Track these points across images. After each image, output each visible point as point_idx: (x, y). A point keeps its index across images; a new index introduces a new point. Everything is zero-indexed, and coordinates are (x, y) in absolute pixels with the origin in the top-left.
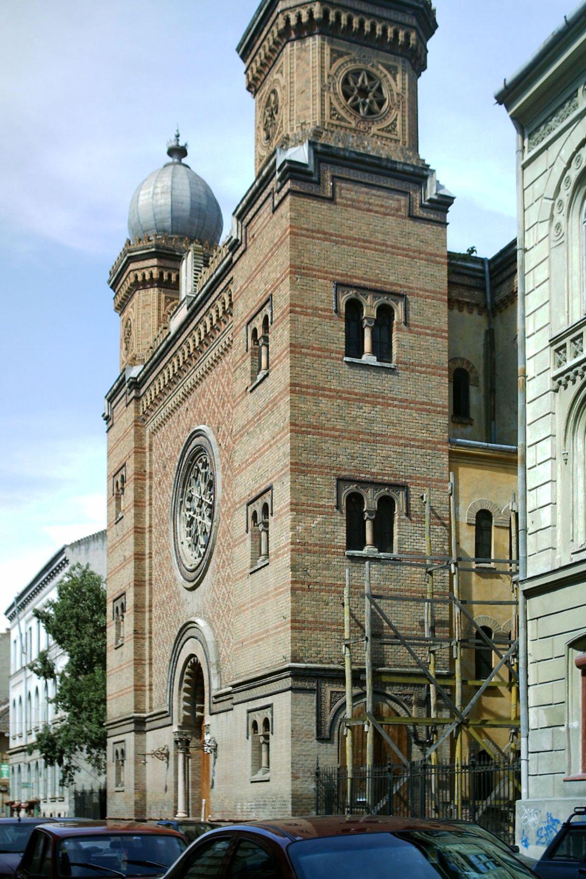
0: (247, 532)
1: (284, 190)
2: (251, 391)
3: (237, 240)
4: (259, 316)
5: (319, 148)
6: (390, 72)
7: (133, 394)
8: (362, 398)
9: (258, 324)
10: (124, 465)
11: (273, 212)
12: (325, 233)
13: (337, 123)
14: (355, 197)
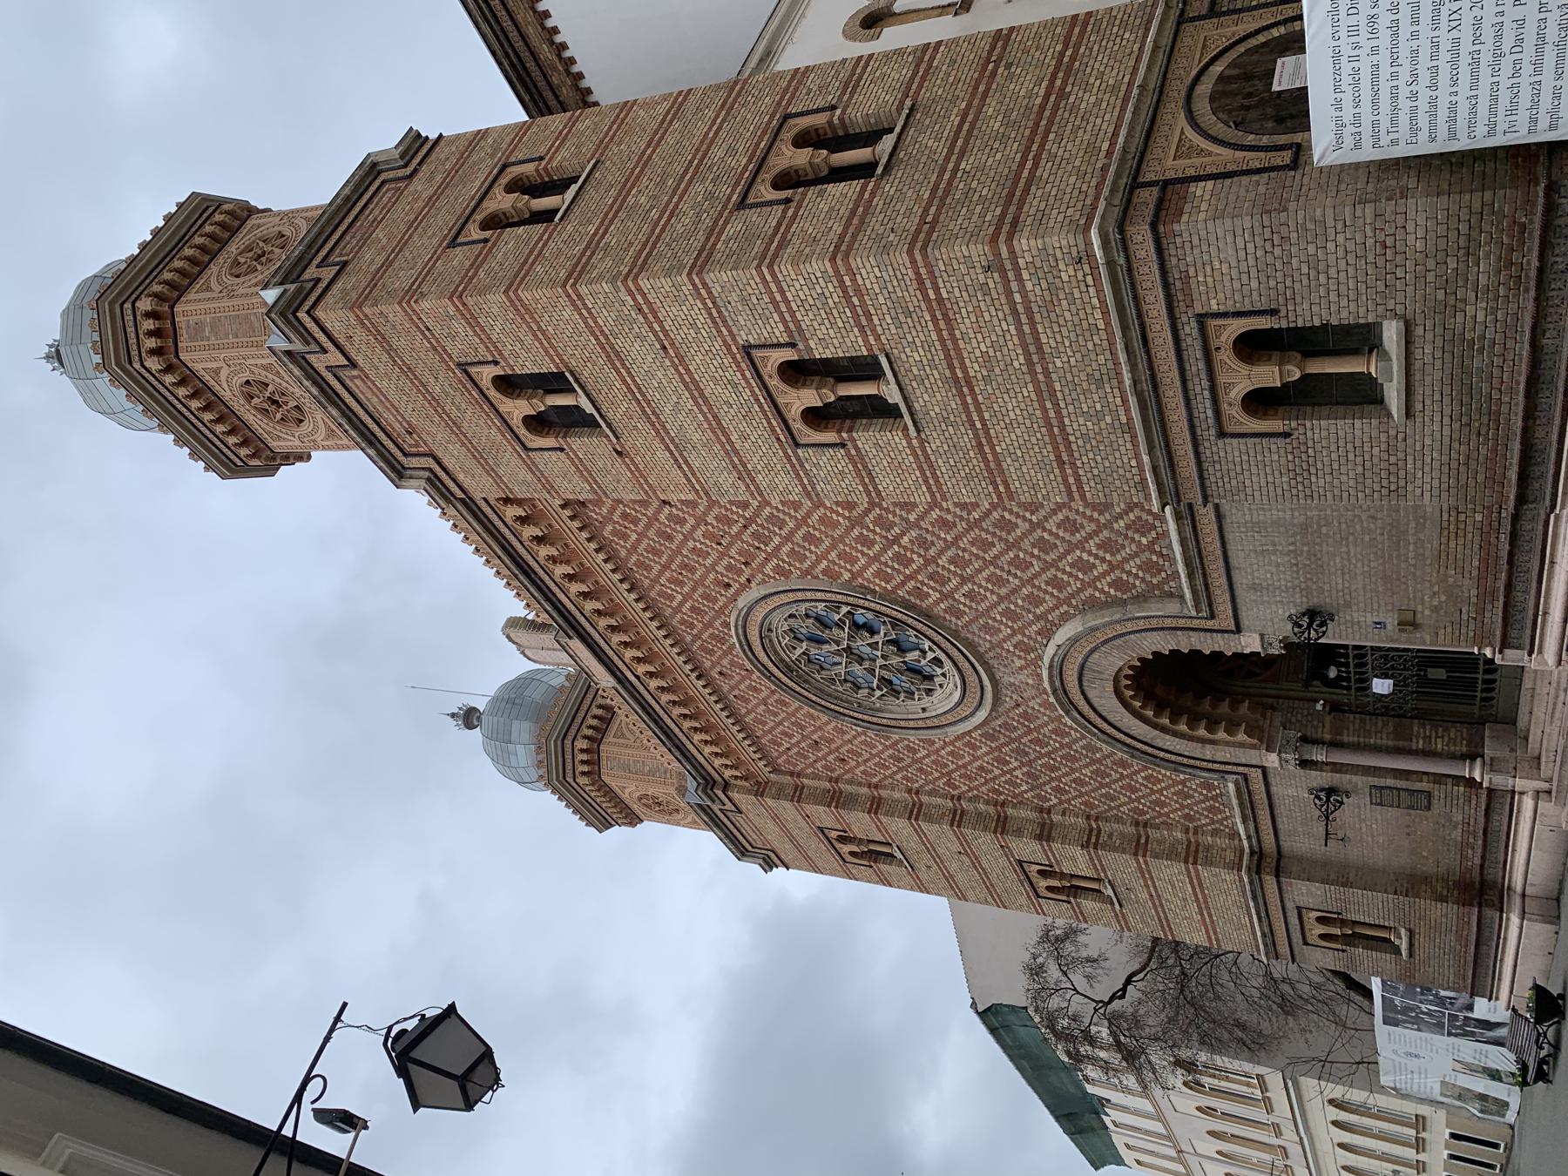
3: (429, 480)
7: (720, 793)
10: (821, 829)
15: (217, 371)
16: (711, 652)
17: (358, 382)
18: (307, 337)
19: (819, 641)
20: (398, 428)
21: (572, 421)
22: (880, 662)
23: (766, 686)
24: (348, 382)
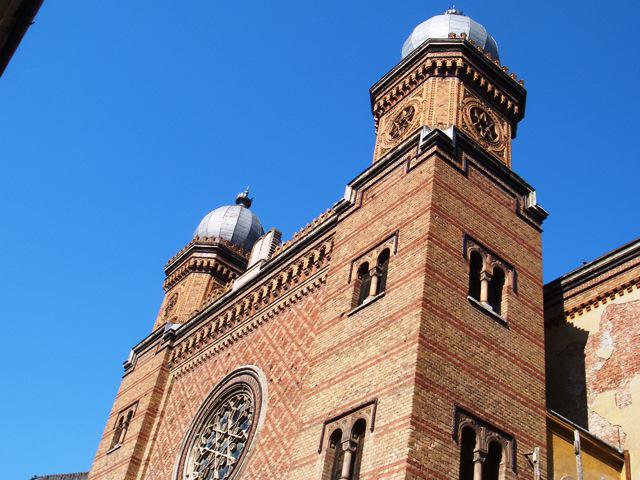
2: (349, 316)
3: (349, 203)
4: (375, 252)
7: (168, 343)
10: (137, 402)
15: (421, 95)
16: (241, 351)
17: (400, 173)
18: (424, 149)
19: (234, 419)
20: (376, 190)
21: (362, 291)
22: (217, 453)
23: (217, 380)
24: (401, 166)
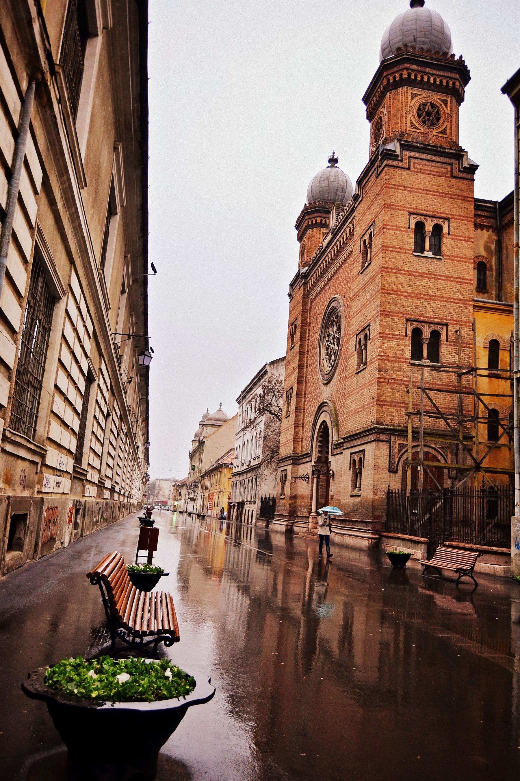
0: (356, 350)
1: (383, 165)
2: (361, 273)
3: (358, 195)
4: (367, 233)
5: (403, 142)
6: (444, 103)
8: (423, 275)
9: (366, 237)
10: (297, 319)
11: (377, 178)
12: (404, 187)
13: (414, 130)
14: (422, 168)
